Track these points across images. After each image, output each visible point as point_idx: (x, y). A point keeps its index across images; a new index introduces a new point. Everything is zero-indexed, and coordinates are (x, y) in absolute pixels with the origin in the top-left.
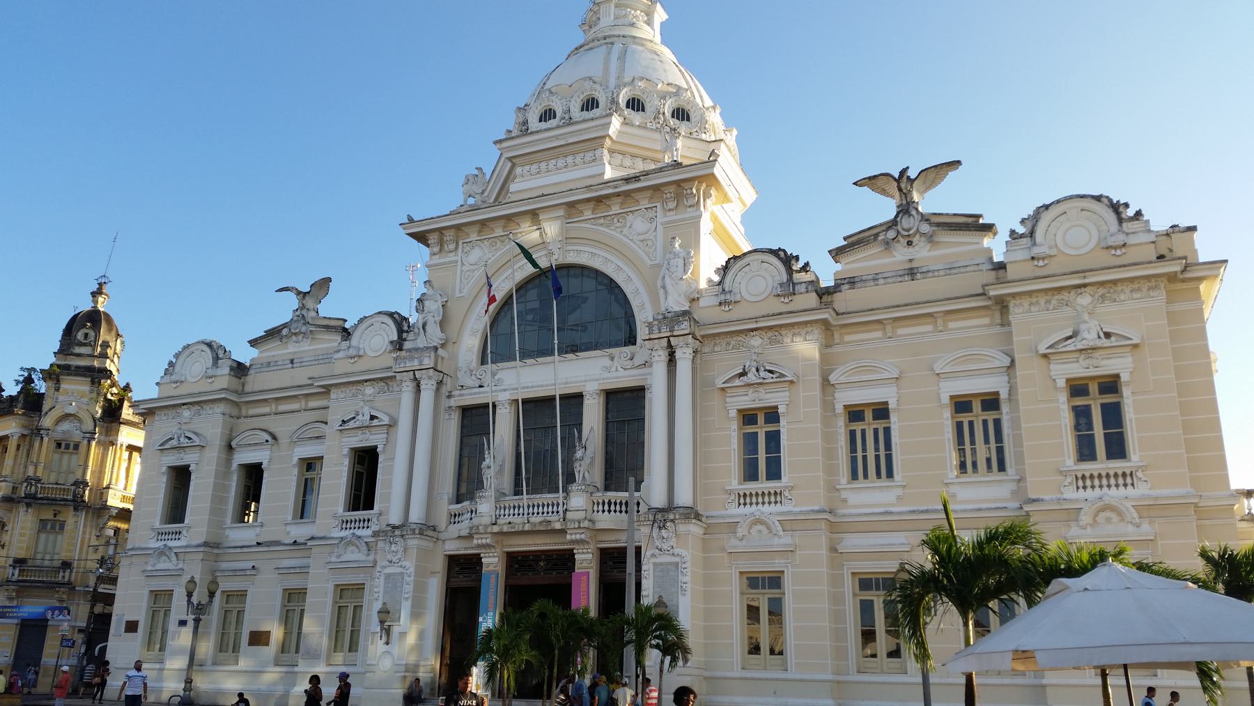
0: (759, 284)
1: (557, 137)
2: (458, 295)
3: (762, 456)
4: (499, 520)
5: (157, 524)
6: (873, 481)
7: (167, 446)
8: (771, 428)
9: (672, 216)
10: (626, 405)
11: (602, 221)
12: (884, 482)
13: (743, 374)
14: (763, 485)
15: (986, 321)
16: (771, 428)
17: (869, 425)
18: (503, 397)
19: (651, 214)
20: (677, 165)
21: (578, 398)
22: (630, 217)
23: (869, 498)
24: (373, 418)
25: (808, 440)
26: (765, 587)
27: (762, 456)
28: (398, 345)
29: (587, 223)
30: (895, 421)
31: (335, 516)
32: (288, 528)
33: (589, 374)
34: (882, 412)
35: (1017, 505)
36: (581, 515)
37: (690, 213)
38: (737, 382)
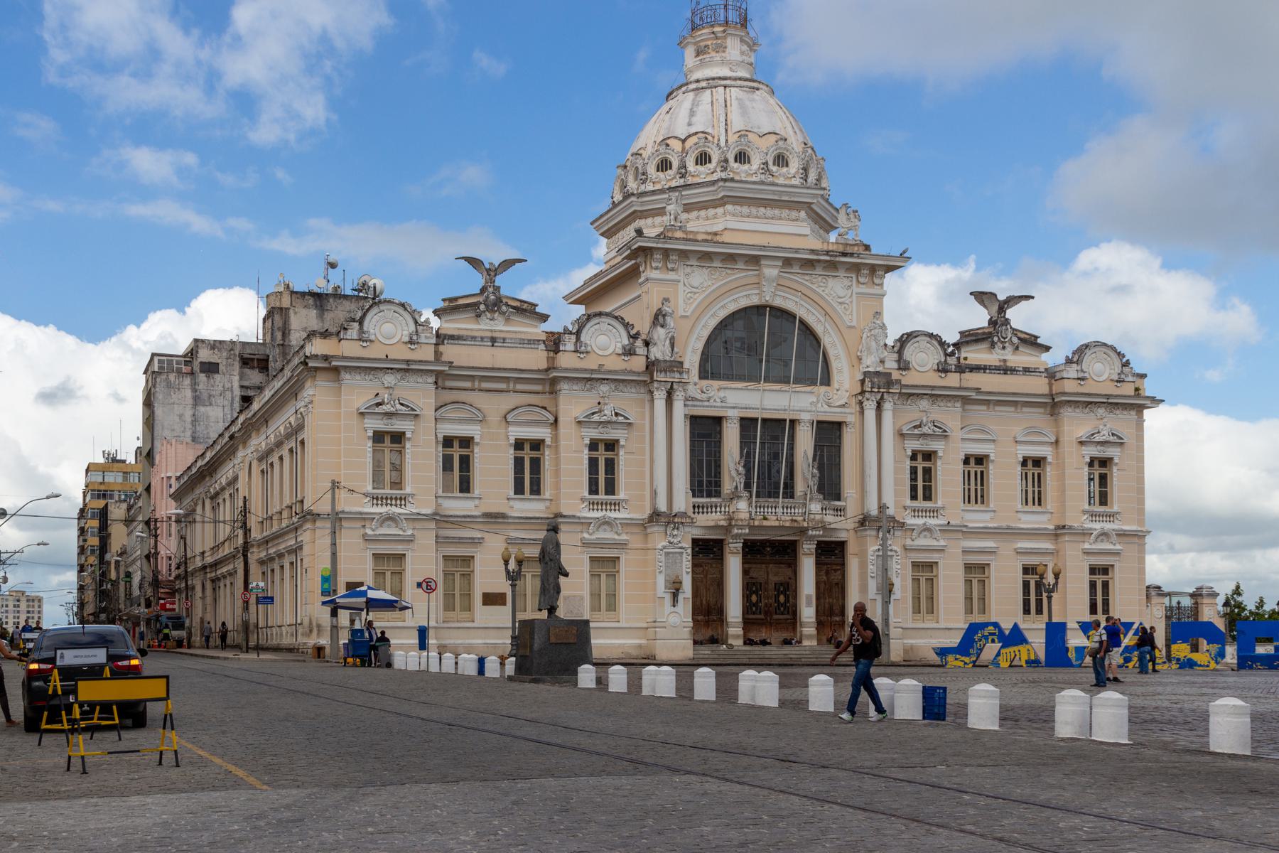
0: (923, 359)
1: (774, 192)
2: (681, 312)
3: (920, 483)
4: (743, 511)
5: (369, 489)
6: (973, 507)
7: (377, 410)
8: (927, 464)
9: (863, 289)
10: (829, 433)
11: (807, 277)
12: (979, 507)
13: (920, 426)
14: (920, 503)
15: (1041, 410)
16: (927, 464)
17: (973, 468)
18: (730, 413)
19: (846, 282)
20: (867, 248)
21: (793, 422)
22: (830, 281)
23: (977, 518)
24: (617, 414)
25: (949, 476)
26: (925, 569)
27: (920, 483)
28: (629, 352)
29: (797, 277)
30: (992, 468)
31: (583, 500)
32: (511, 503)
33: (799, 404)
34: (980, 460)
35: (1052, 527)
36: (818, 517)
37: (876, 290)
38: (916, 431)
